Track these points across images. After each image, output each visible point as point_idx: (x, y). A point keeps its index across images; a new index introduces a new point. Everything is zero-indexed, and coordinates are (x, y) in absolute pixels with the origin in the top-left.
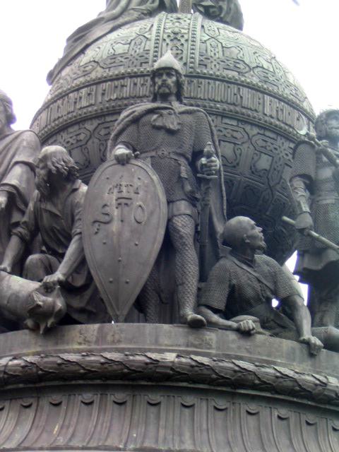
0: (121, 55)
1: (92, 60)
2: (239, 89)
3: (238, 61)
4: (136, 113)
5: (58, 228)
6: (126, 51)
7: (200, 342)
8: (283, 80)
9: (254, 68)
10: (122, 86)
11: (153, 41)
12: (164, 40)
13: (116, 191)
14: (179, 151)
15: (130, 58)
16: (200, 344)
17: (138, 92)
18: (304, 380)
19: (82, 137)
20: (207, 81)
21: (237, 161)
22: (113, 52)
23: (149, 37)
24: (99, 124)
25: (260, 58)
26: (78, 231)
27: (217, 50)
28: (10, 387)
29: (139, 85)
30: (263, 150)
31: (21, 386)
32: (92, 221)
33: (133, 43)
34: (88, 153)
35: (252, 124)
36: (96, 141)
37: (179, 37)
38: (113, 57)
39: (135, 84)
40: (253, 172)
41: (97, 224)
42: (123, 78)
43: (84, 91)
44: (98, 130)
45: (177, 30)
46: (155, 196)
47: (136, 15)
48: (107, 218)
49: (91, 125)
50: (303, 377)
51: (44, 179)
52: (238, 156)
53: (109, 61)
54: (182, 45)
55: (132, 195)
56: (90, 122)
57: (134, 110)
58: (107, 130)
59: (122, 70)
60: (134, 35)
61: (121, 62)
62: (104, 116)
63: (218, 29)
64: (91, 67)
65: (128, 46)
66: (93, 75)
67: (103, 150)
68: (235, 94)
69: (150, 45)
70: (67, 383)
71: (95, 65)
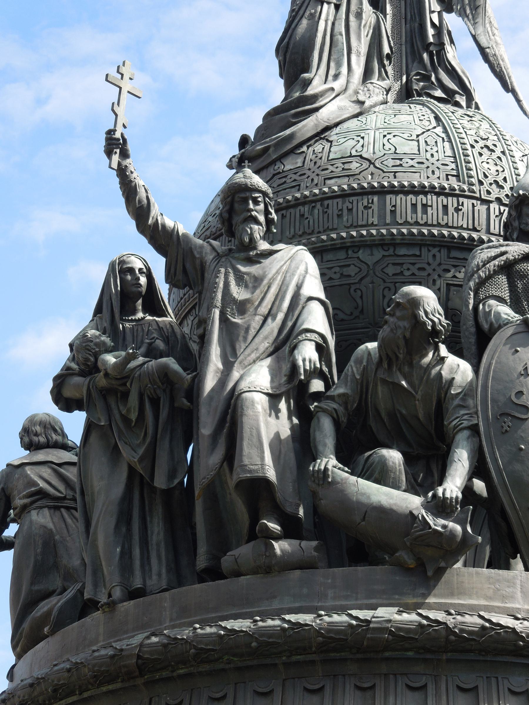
1: (354, 153)
5: (404, 412)
15: (427, 164)
19: (352, 271)
22: (393, 149)
24: (384, 256)
26: (465, 424)
28: (387, 654)
31: (410, 654)
34: (361, 297)
37: (489, 143)
42: (425, 194)
45: (482, 134)
49: (372, 255)
53: (391, 163)
54: (499, 158)
56: (368, 251)
57: (503, 249)
58: (399, 267)
61: (412, 166)
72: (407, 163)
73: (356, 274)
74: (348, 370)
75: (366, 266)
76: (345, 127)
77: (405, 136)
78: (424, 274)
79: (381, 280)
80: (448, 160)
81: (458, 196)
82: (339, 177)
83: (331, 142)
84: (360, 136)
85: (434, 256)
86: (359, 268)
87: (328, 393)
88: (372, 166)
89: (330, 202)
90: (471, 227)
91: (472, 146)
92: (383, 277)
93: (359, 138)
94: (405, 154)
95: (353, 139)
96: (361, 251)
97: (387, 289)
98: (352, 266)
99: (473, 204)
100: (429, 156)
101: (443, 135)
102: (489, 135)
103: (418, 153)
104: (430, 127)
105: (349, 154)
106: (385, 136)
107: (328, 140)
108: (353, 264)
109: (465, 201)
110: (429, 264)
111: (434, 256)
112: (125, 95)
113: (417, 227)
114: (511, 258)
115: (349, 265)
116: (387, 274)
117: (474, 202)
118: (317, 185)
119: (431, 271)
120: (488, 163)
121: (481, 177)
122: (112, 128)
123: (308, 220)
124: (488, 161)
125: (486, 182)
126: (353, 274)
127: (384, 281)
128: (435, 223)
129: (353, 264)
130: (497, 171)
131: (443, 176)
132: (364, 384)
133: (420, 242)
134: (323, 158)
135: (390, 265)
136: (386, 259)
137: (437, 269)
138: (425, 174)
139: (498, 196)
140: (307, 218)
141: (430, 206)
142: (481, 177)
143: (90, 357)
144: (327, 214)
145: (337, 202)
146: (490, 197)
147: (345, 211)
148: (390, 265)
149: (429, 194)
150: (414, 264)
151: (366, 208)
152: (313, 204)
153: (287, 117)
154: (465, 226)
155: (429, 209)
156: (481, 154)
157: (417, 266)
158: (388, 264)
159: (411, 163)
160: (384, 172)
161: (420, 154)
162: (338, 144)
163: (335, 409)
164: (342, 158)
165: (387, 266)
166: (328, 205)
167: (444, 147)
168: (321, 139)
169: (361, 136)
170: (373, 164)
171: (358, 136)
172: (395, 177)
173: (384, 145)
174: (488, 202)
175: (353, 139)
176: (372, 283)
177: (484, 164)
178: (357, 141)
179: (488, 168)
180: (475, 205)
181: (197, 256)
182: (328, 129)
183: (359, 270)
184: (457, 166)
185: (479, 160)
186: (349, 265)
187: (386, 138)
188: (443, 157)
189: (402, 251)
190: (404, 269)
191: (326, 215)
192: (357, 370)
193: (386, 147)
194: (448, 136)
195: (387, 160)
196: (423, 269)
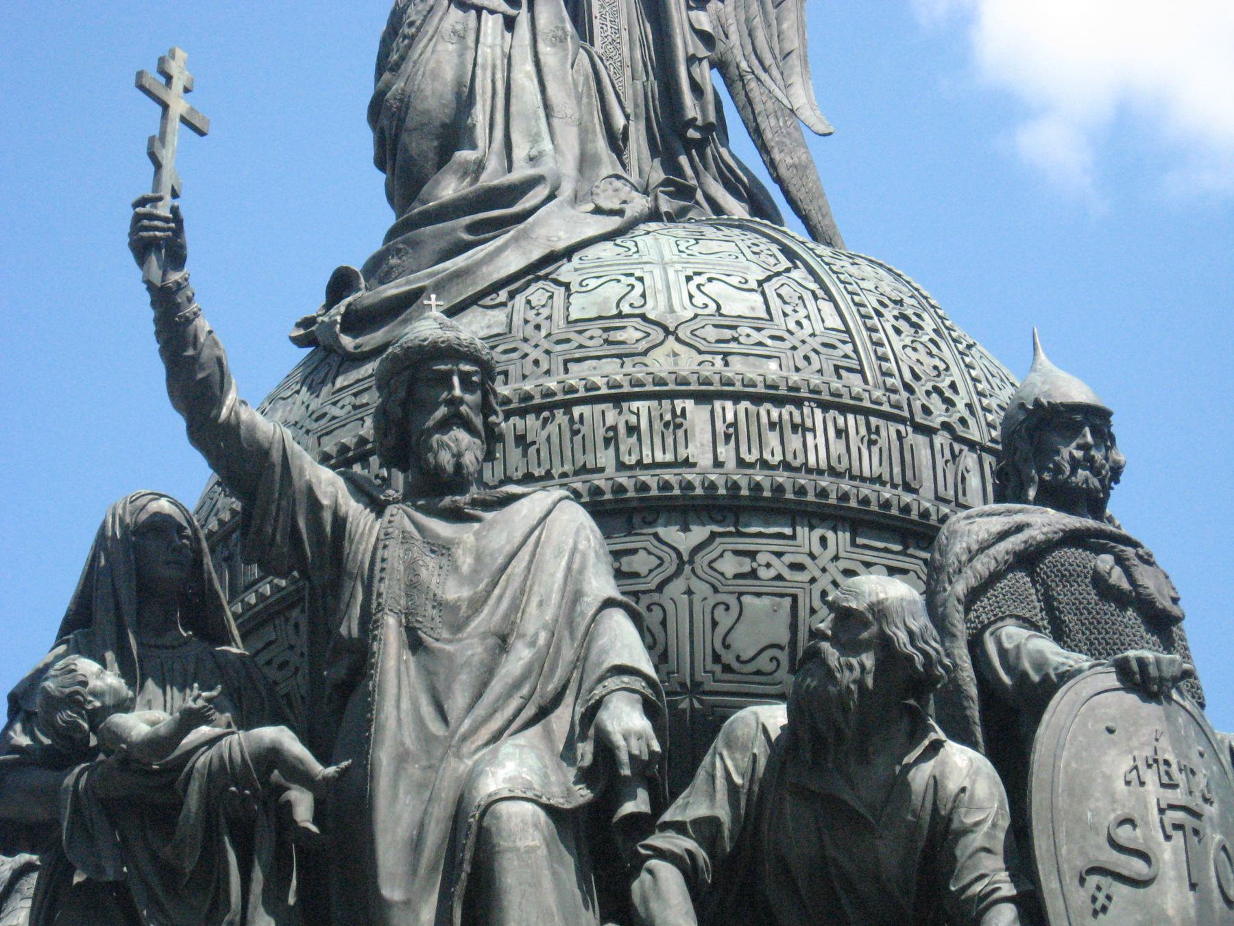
1: (626, 309)
10: (795, 428)
13: (1150, 777)
17: (855, 464)
19: (641, 562)
22: (713, 307)
24: (713, 535)
29: (852, 430)
32: (1082, 864)
34: (664, 623)
36: (701, 589)
37: (909, 312)
39: (839, 433)
42: (798, 403)
43: (641, 406)
48: (1137, 867)
51: (860, 683)
53: (712, 334)
55: (1196, 803)
57: (1019, 518)
58: (747, 560)
61: (760, 344)
64: (639, 335)
66: (661, 363)
72: (748, 336)
73: (651, 571)
74: (713, 764)
75: (674, 555)
76: (590, 257)
77: (735, 280)
78: (803, 577)
79: (708, 585)
80: (833, 338)
81: (866, 412)
82: (599, 358)
83: (567, 286)
84: (632, 275)
85: (823, 540)
86: (659, 558)
87: (667, 817)
88: (671, 338)
89: (585, 410)
90: (898, 479)
91: (879, 314)
93: (632, 280)
95: (619, 281)
97: (722, 607)
98: (642, 553)
99: (898, 432)
100: (792, 326)
101: (814, 286)
103: (768, 317)
104: (781, 268)
105: (614, 312)
106: (689, 279)
107: (557, 283)
108: (645, 549)
109: (881, 423)
110: (812, 556)
111: (823, 540)
112: (175, 124)
113: (786, 474)
114: (1040, 537)
116: (722, 574)
117: (901, 428)
118: (548, 372)
119: (817, 573)
120: (915, 349)
121: (908, 376)
122: (148, 193)
123: (536, 446)
124: (914, 345)
125: (920, 388)
126: (643, 571)
127: (716, 590)
128: (823, 464)
129: (645, 549)
130: (936, 368)
131: (829, 369)
134: (555, 317)
135: (728, 555)
136: (718, 540)
137: (831, 567)
138: (791, 363)
139: (946, 419)
140: (534, 443)
141: (809, 430)
142: (908, 376)
143: (81, 721)
144: (580, 436)
145: (603, 412)
146: (931, 421)
147: (622, 430)
148: (728, 555)
149: (806, 403)
150: (779, 555)
151: (667, 425)
152: (546, 414)
153: (454, 230)
154: (886, 477)
155: (809, 436)
156: (898, 331)
157: (788, 559)
158: (724, 551)
159: (756, 337)
160: (700, 352)
161: (771, 319)
162: (584, 289)
163: (689, 852)
164: (600, 318)
165: (721, 556)
166: (581, 416)
167: (819, 310)
168: (538, 279)
169: (636, 275)
170: (674, 333)
171: (627, 275)
172: (727, 364)
173: (691, 297)
174: (928, 431)
175: (619, 281)
176: (689, 592)
177: (908, 350)
178: (628, 285)
179: (918, 361)
180: (904, 434)
181: (325, 502)
182: (552, 258)
183: (658, 562)
184: (856, 351)
185: (897, 342)
186: (634, 551)
187: (693, 285)
188: (823, 329)
190: (759, 565)
191: (578, 438)
192: (737, 767)
193: (699, 299)
194: (824, 287)
195: (703, 327)
196: (797, 567)
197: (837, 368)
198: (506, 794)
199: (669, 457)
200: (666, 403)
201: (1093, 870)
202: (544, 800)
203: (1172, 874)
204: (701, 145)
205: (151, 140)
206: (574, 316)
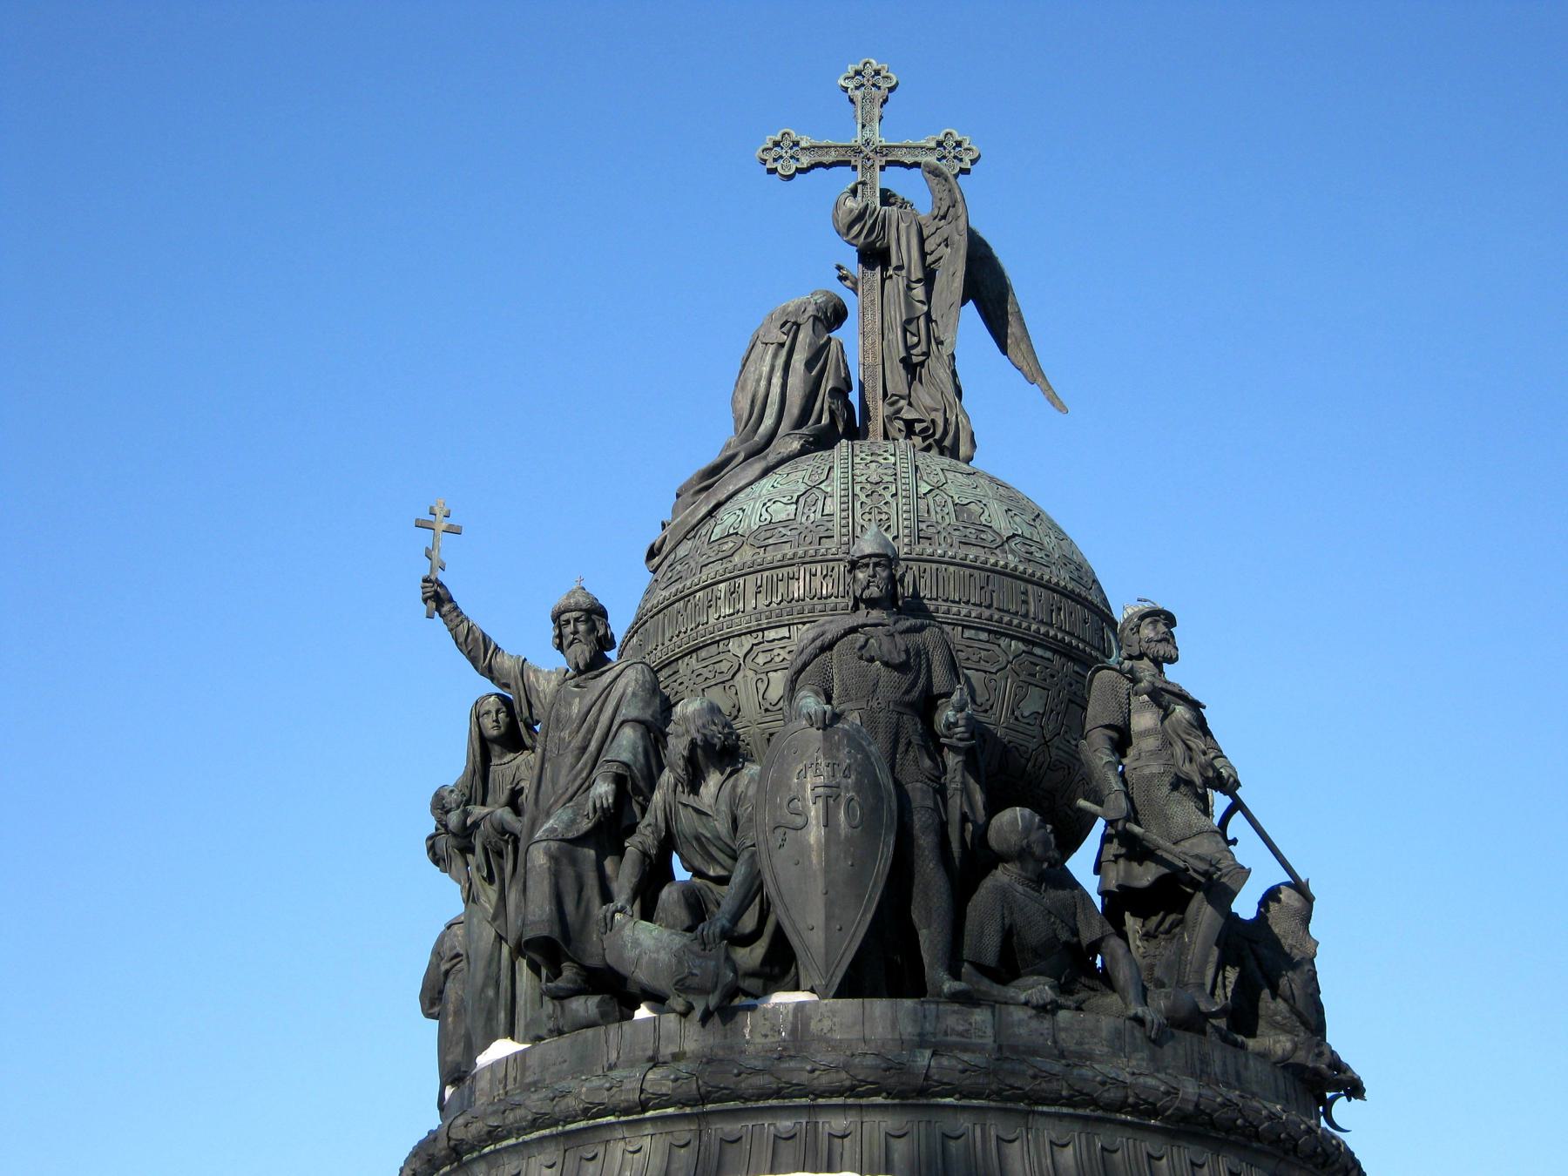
0: (785, 523)
1: (731, 532)
2: (988, 576)
3: (982, 528)
4: (829, 636)
5: (709, 835)
6: (792, 517)
7: (967, 1027)
8: (1057, 556)
9: (1008, 538)
11: (837, 494)
12: (854, 495)
14: (907, 698)
15: (801, 528)
16: (967, 1031)
18: (1145, 1086)
20: (934, 566)
21: (990, 702)
23: (829, 489)
24: (753, 645)
25: (1017, 519)
26: (749, 843)
27: (946, 510)
30: (1030, 679)
31: (670, 1110)
33: (802, 500)
35: (1013, 637)
36: (751, 674)
38: (771, 525)
40: (1016, 719)
41: (781, 831)
43: (722, 586)
44: (749, 659)
45: (875, 478)
46: (876, 784)
47: (796, 445)
48: (799, 821)
50: (1141, 1080)
52: (992, 693)
58: (768, 654)
59: (788, 550)
60: (803, 488)
62: (763, 630)
63: (942, 470)
64: (733, 544)
65: (794, 506)
67: (762, 687)
68: (982, 588)
69: (832, 506)
70: (750, 1104)
71: (739, 540)
77: (785, 500)
92: (755, 668)
93: (740, 513)
94: (780, 522)
96: (731, 644)
100: (804, 520)
102: (884, 477)
106: (765, 504)
115: (721, 661)
120: (870, 513)
132: (668, 809)
133: (787, 622)
159: (784, 531)
171: (739, 509)
173: (761, 515)
186: (721, 661)
189: (771, 634)
193: (763, 519)
197: (820, 538)
198: (544, 838)
199: (732, 611)
200: (732, 582)
201: (776, 828)
202: (560, 836)
203: (814, 822)
204: (922, 364)
205: (427, 548)
206: (712, 540)
